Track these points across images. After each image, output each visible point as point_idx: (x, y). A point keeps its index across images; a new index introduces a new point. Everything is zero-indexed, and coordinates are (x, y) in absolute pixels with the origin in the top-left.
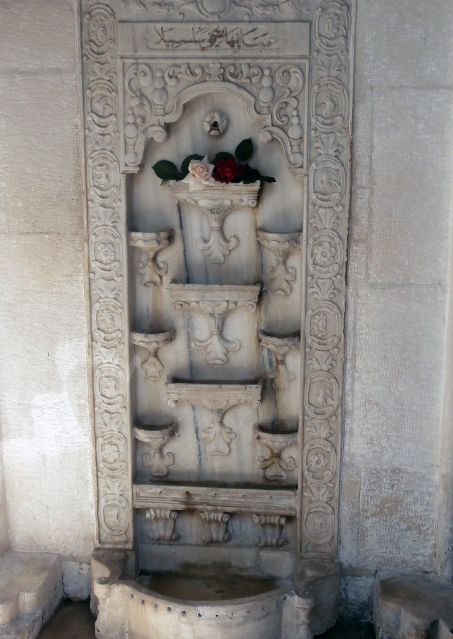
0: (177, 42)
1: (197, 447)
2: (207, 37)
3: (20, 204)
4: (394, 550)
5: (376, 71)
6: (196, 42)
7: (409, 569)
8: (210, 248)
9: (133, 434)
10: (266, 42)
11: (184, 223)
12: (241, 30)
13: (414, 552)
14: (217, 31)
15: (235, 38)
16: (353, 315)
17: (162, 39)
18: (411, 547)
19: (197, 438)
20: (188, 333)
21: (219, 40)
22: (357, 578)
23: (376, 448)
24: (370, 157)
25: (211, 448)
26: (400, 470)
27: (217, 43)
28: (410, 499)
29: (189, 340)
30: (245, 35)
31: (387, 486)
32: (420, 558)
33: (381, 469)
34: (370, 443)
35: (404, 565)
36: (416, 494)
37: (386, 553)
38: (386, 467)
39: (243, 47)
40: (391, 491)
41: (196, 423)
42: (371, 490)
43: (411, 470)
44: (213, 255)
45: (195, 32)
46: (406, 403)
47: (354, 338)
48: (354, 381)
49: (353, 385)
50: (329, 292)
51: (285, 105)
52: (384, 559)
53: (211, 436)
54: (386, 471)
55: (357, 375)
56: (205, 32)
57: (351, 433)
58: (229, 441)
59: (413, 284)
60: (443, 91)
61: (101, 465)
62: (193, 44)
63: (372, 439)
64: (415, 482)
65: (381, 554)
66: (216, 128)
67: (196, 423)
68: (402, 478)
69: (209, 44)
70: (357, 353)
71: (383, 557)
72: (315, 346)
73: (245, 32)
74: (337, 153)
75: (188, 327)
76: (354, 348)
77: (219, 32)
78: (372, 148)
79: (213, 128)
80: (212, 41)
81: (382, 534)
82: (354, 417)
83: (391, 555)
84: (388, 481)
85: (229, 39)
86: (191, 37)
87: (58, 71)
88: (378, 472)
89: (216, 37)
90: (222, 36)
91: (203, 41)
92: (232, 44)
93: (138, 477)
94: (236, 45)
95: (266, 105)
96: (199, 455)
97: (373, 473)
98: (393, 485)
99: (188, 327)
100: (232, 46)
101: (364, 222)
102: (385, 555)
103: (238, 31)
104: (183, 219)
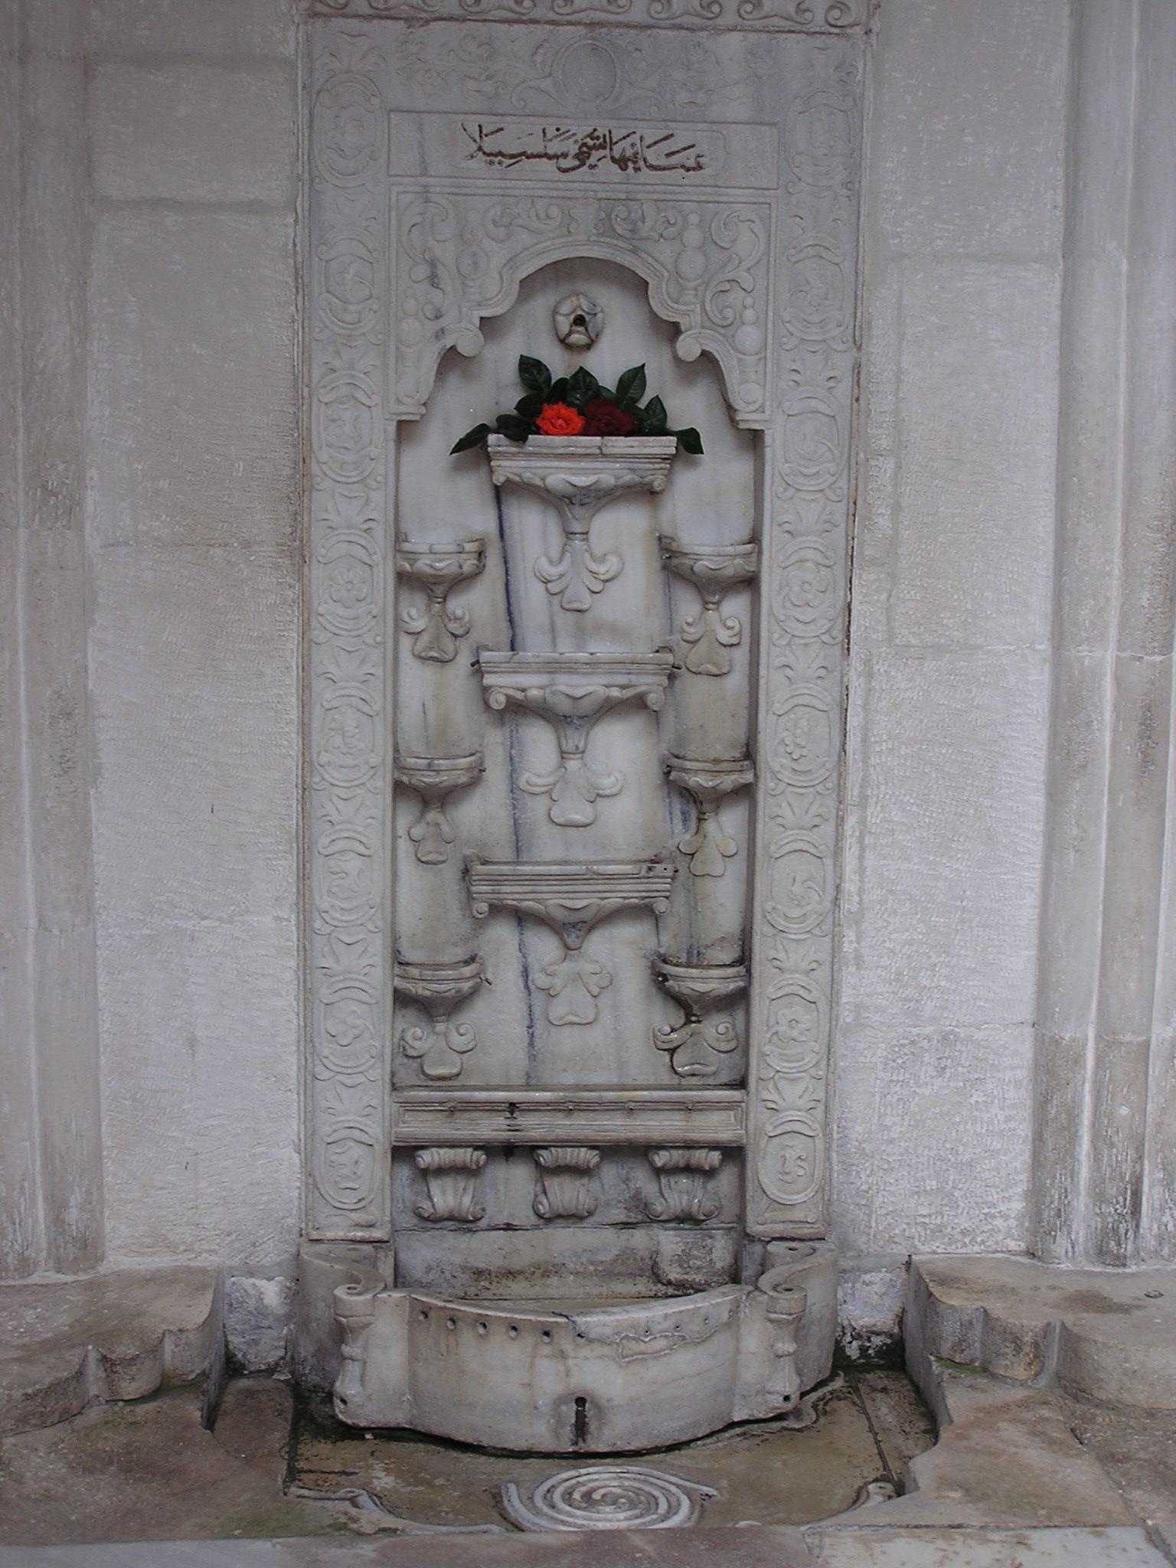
0: (512, 156)
1: (525, 1008)
2: (574, 149)
3: (164, 484)
5: (907, 223)
6: (550, 157)
7: (976, 1248)
8: (562, 576)
10: (691, 163)
11: (506, 525)
12: (641, 138)
13: (986, 1211)
14: (591, 136)
15: (629, 153)
16: (862, 715)
17: (480, 149)
18: (980, 1200)
19: (527, 987)
20: (511, 759)
21: (596, 155)
22: (867, 1277)
23: (910, 992)
24: (896, 394)
26: (957, 1035)
27: (592, 160)
28: (977, 1097)
29: (513, 774)
30: (649, 147)
31: (931, 1071)
32: (999, 1222)
33: (918, 1035)
34: (897, 981)
35: (967, 1240)
36: (989, 1086)
37: (930, 1216)
38: (928, 1030)
39: (645, 169)
42: (898, 1081)
43: (978, 1035)
44: (567, 593)
45: (549, 136)
46: (968, 893)
47: (865, 762)
48: (862, 850)
49: (861, 858)
50: (815, 665)
51: (727, 286)
53: (558, 982)
55: (869, 840)
56: (568, 138)
57: (858, 958)
58: (595, 991)
59: (979, 647)
60: (1036, 266)
62: (545, 160)
63: (899, 973)
64: (986, 1060)
66: (581, 329)
68: (961, 1053)
69: (577, 163)
70: (869, 792)
72: (786, 776)
73: (648, 141)
74: (831, 384)
75: (512, 747)
76: (865, 783)
77: (598, 138)
78: (898, 376)
79: (575, 328)
80: (582, 157)
81: (920, 1174)
82: (864, 926)
83: (938, 1221)
84: (933, 1061)
85: (617, 156)
86: (539, 149)
87: (254, 207)
88: (913, 1042)
89: (591, 148)
90: (602, 147)
91: (565, 155)
92: (622, 162)
94: (630, 165)
95: (692, 284)
97: (903, 1045)
98: (944, 1069)
99: (512, 747)
100: (624, 168)
101: (884, 522)
102: (927, 1220)
103: (635, 138)
104: (505, 517)
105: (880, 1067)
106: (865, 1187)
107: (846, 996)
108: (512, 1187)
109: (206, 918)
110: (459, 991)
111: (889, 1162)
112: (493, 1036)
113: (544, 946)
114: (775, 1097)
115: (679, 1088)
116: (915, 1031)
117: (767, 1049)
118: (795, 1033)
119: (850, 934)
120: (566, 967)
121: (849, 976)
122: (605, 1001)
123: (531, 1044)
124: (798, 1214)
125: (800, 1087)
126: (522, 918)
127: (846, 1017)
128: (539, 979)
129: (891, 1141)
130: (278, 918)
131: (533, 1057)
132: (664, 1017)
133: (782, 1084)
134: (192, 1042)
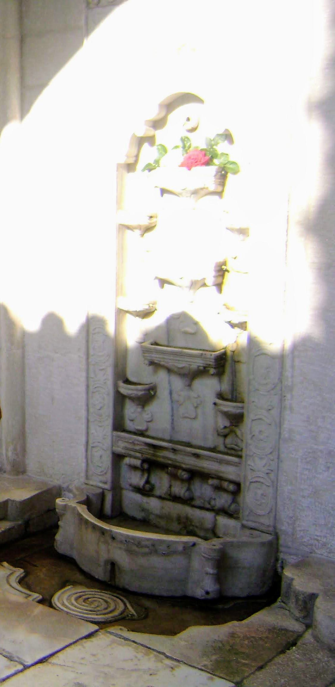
4: (328, 535)
9: (116, 386)
25: (182, 411)
37: (320, 536)
38: (321, 447)
40: (326, 474)
41: (170, 386)
42: (307, 469)
52: (319, 542)
54: (321, 451)
57: (291, 409)
61: (91, 410)
65: (316, 537)
67: (170, 386)
71: (318, 540)
83: (325, 540)
93: (119, 425)
96: (172, 416)
97: (309, 453)
102: (319, 538)
105: (299, 460)
106: (291, 515)
107: (286, 425)
108: (162, 482)
109: (57, 353)
110: (137, 395)
111: (302, 506)
112: (158, 417)
113: (178, 383)
114: (253, 465)
115: (227, 454)
116: (316, 447)
117: (250, 441)
118: (261, 437)
119: (288, 396)
120: (183, 394)
121: (287, 415)
122: (199, 411)
123: (172, 423)
124: (262, 520)
125: (264, 462)
126: (169, 370)
127: (285, 434)
128: (175, 396)
129: (304, 497)
130: (79, 356)
131: (173, 428)
132: (222, 422)
133: (256, 459)
134: (53, 399)
